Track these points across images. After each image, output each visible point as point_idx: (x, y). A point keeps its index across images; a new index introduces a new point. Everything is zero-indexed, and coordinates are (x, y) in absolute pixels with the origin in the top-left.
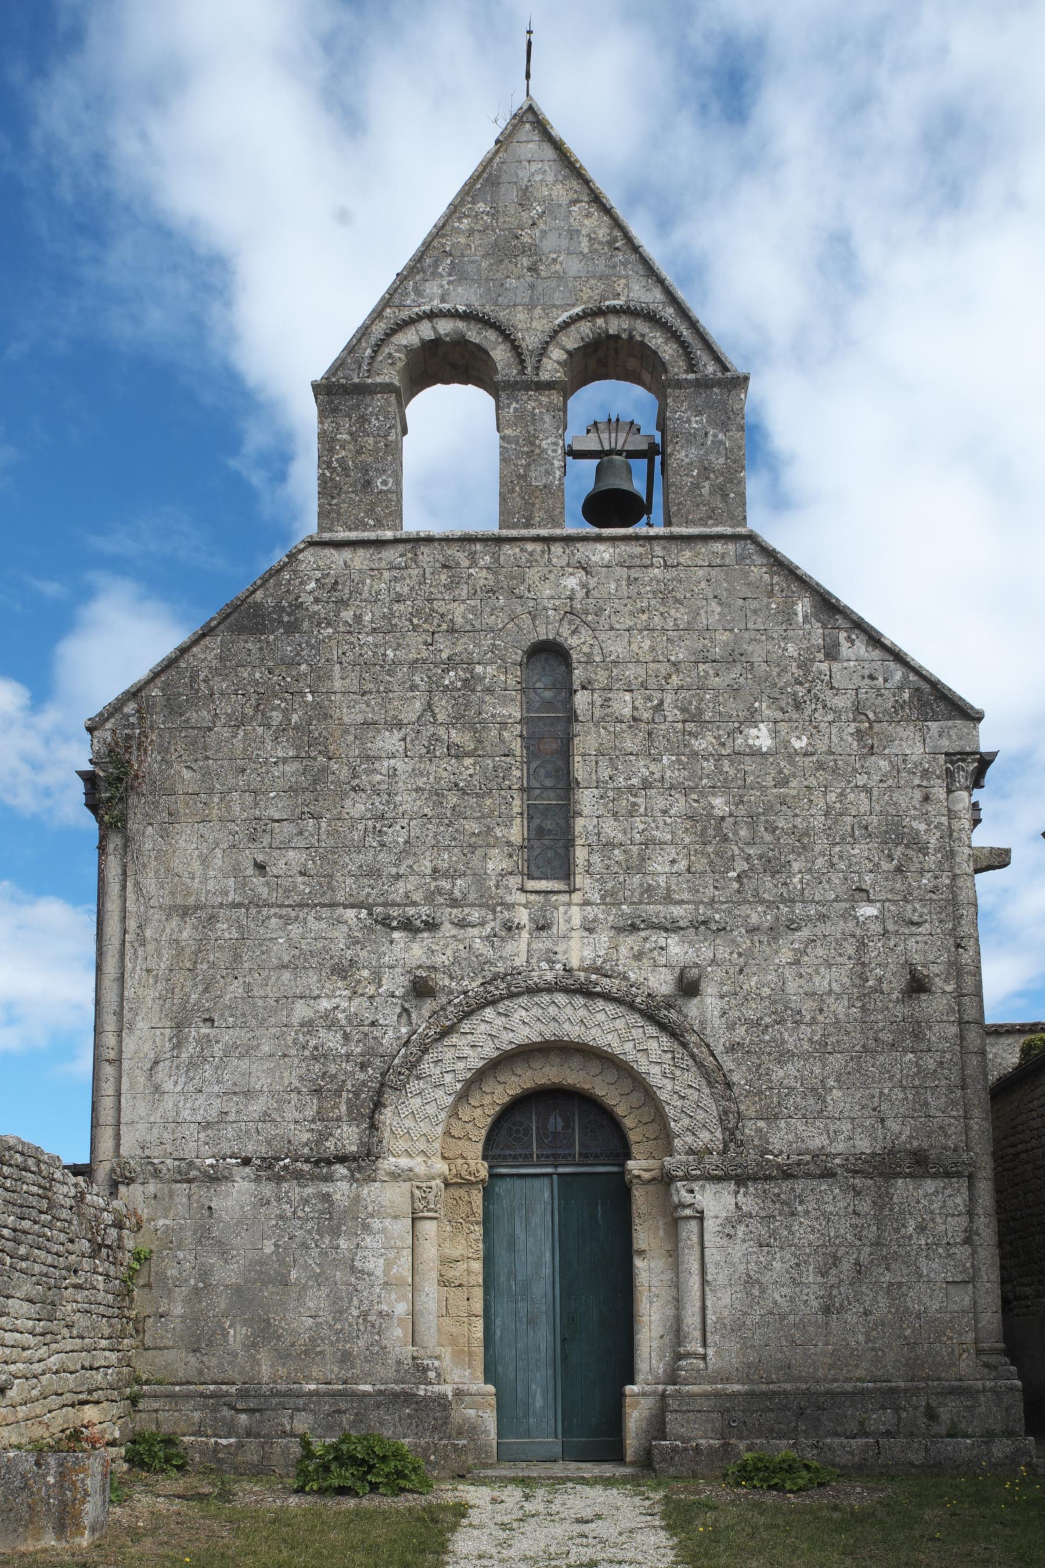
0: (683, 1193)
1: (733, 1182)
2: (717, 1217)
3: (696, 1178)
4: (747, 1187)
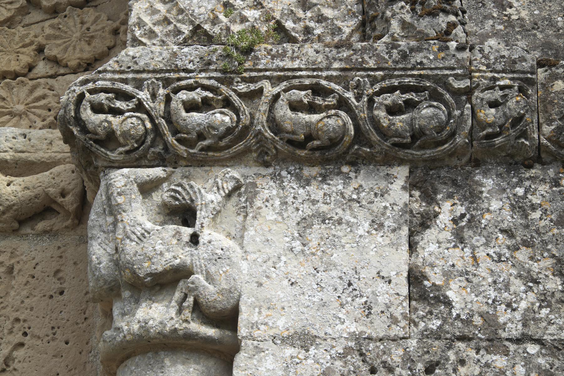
0: (139, 214)
1: (401, 173)
2: (304, 340)
3: (210, 151)
4: (472, 197)
